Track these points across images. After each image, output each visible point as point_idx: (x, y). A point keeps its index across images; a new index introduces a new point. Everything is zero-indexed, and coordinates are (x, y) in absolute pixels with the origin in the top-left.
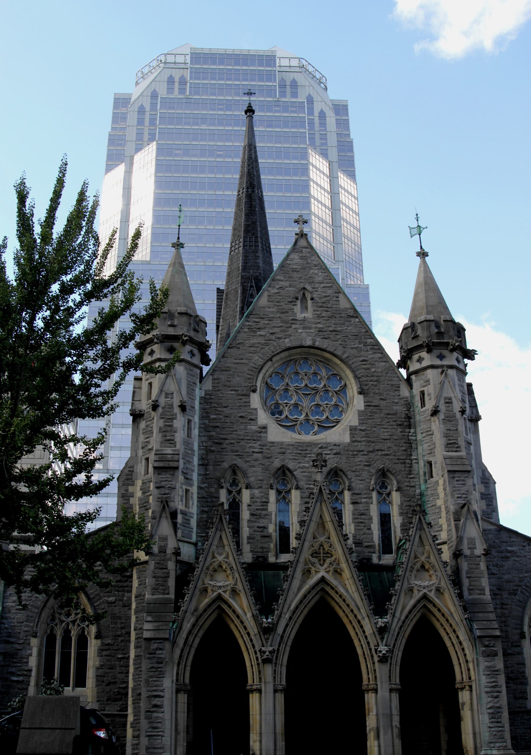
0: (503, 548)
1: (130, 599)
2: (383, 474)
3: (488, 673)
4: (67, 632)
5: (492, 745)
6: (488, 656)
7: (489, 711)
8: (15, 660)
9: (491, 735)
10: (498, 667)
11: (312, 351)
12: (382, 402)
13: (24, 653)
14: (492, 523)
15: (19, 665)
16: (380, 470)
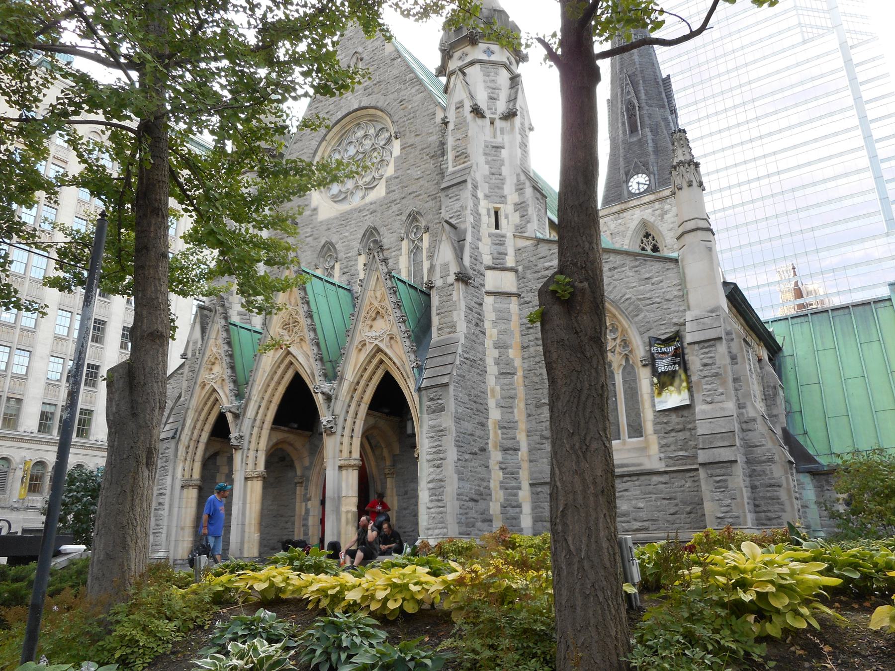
0: (540, 266)
2: (413, 217)
3: (433, 434)
5: (430, 532)
6: (434, 412)
7: (431, 486)
9: (429, 518)
10: (444, 426)
11: (359, 113)
12: (419, 138)
14: (527, 238)
16: (410, 215)
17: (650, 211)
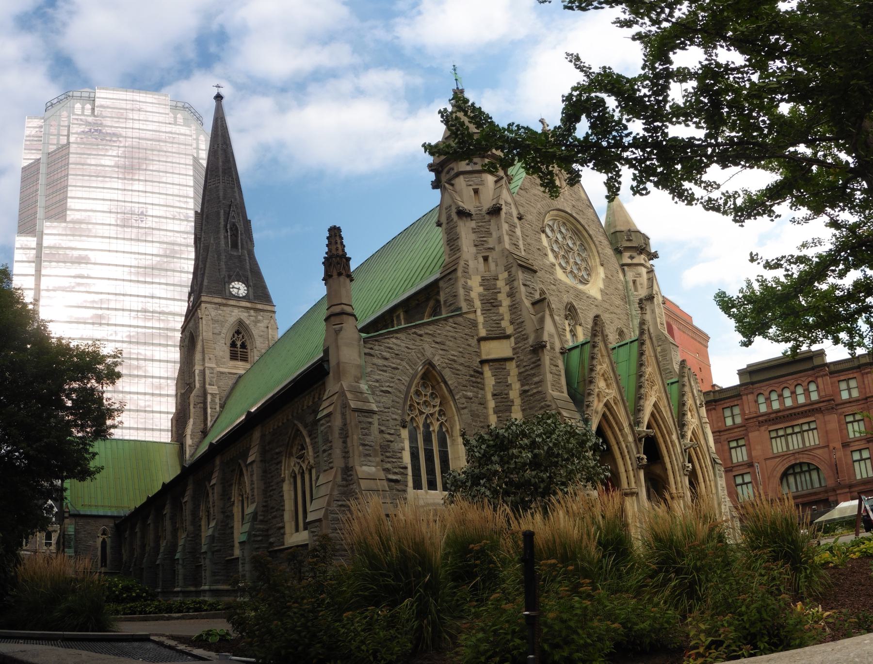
1: (484, 397)
4: (427, 426)
8: (388, 454)
13: (395, 446)
15: (394, 460)
17: (247, 314)
